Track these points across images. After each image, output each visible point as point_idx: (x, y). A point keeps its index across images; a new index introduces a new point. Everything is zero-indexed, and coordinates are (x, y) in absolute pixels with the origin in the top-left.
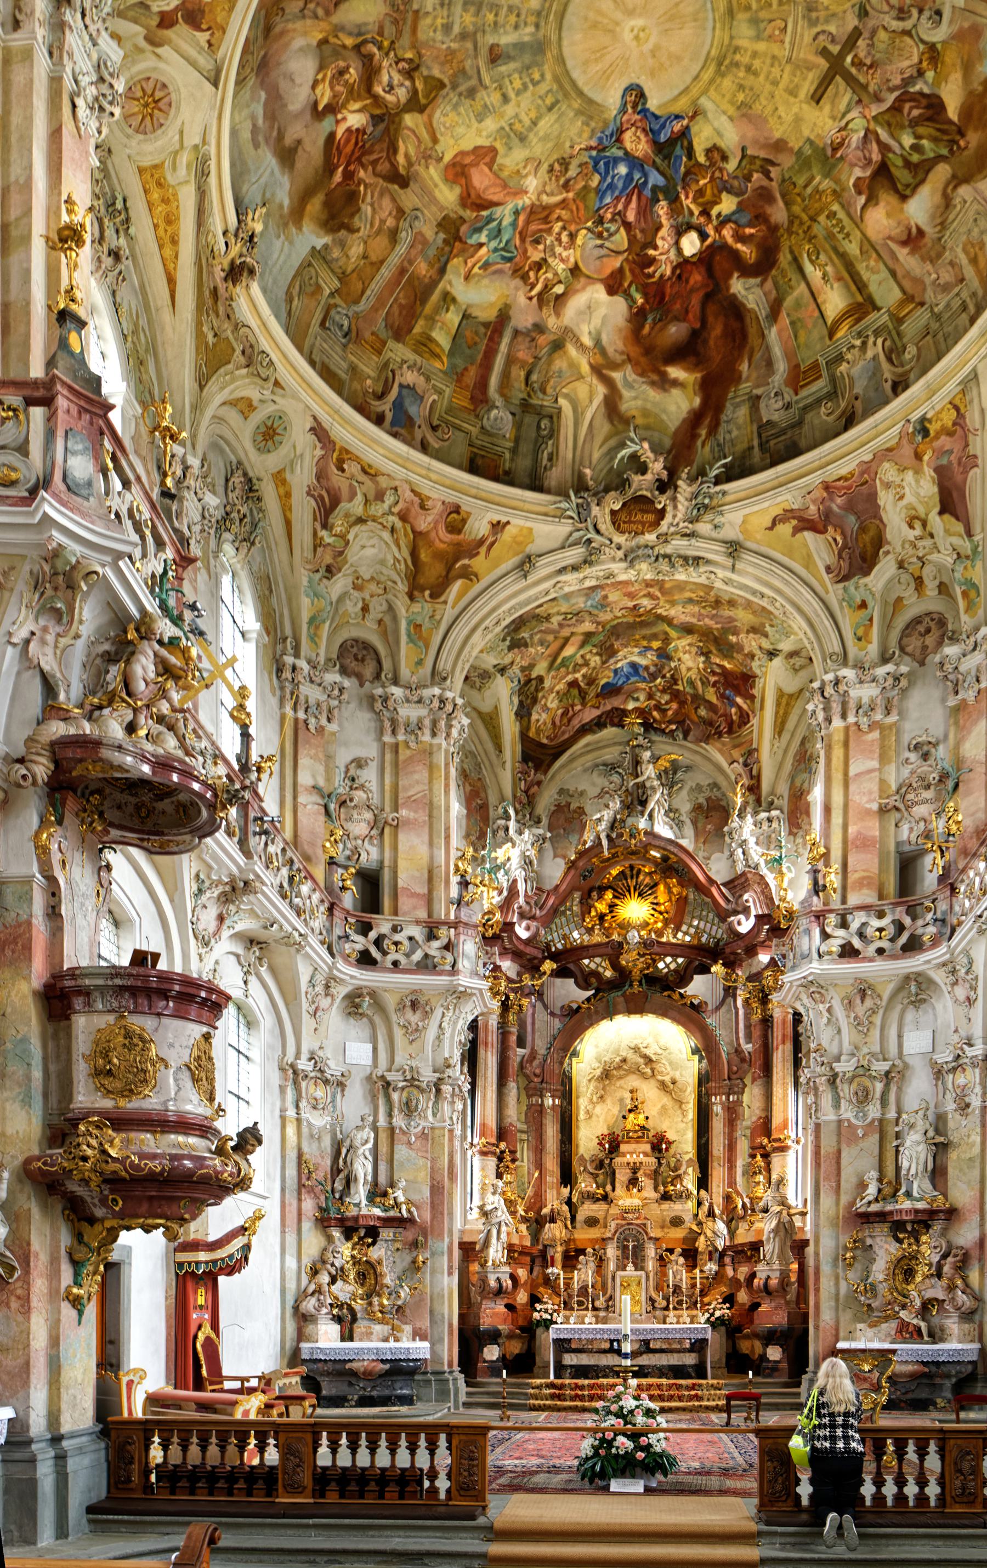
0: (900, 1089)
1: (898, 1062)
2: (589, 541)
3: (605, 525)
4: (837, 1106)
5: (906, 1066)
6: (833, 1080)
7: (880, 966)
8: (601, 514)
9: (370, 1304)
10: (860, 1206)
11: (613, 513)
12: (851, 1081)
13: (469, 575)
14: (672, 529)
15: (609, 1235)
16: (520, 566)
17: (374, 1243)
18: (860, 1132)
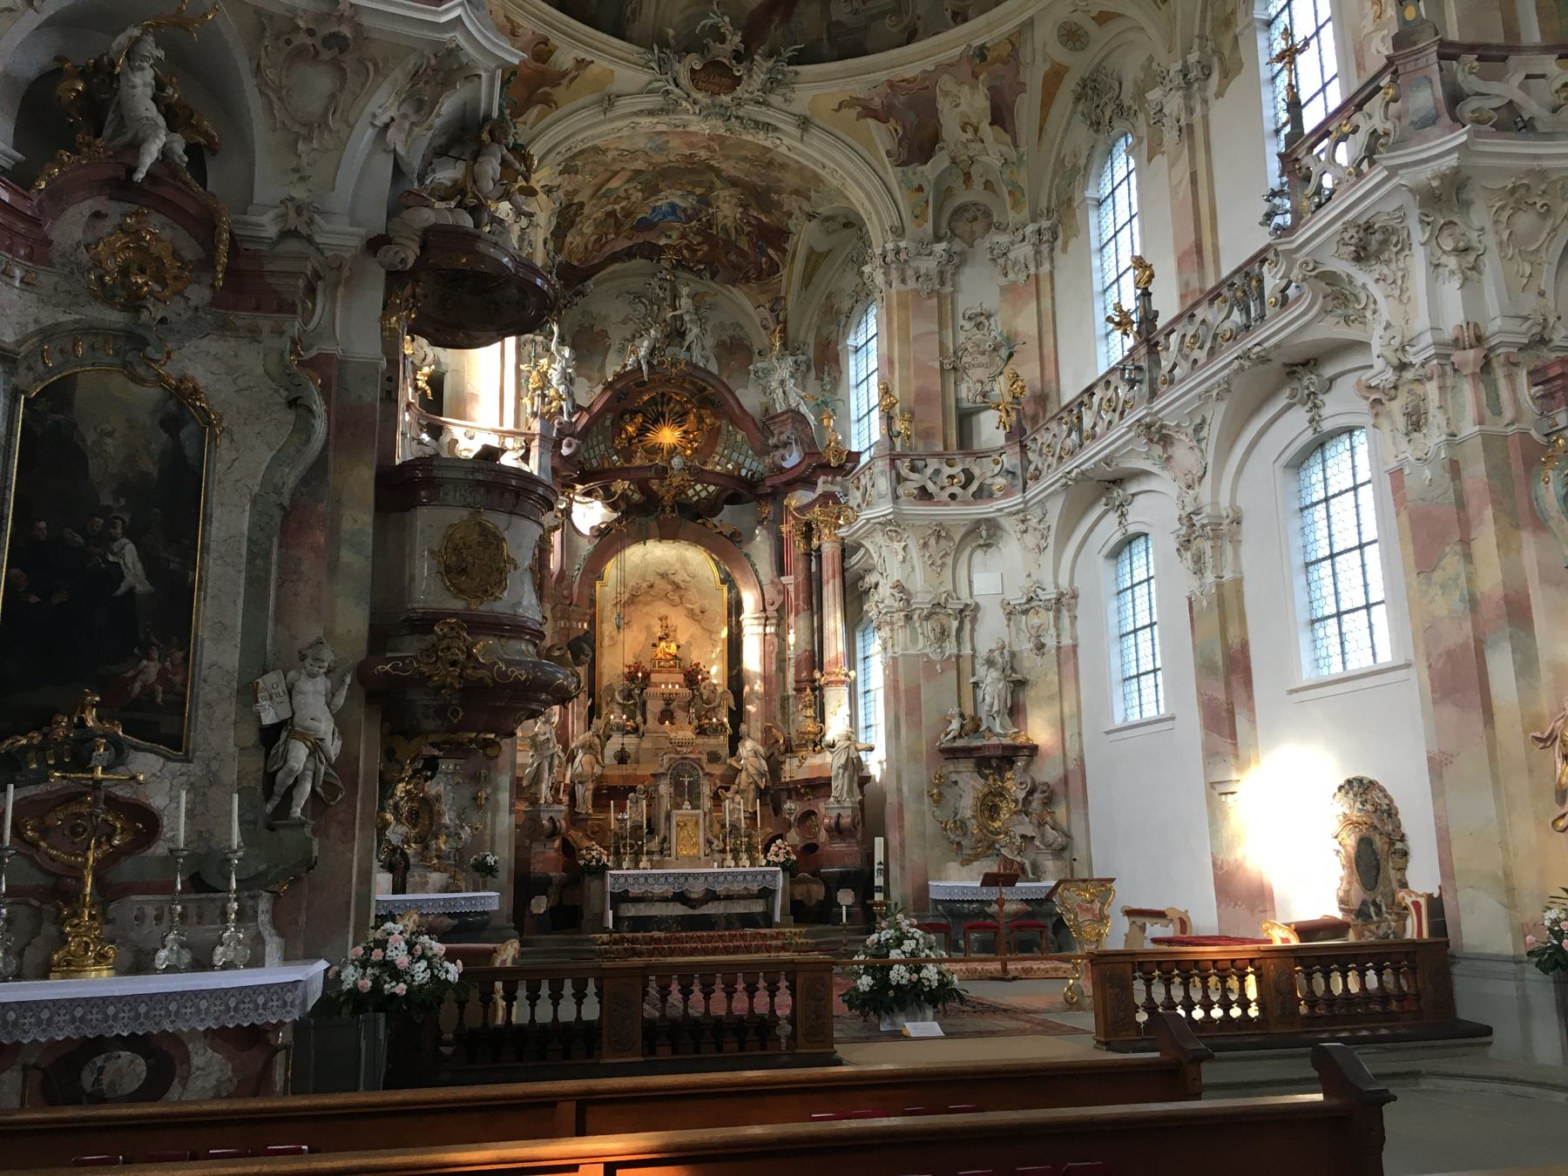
0: (973, 630)
1: (969, 601)
2: (667, 92)
3: (684, 80)
4: (914, 641)
5: (977, 608)
6: (908, 618)
7: (954, 509)
8: (682, 70)
9: (427, 848)
10: (945, 741)
11: (693, 71)
12: (927, 618)
13: (548, 102)
14: (747, 95)
15: (661, 770)
16: (599, 102)
17: (432, 778)
18: (938, 667)
